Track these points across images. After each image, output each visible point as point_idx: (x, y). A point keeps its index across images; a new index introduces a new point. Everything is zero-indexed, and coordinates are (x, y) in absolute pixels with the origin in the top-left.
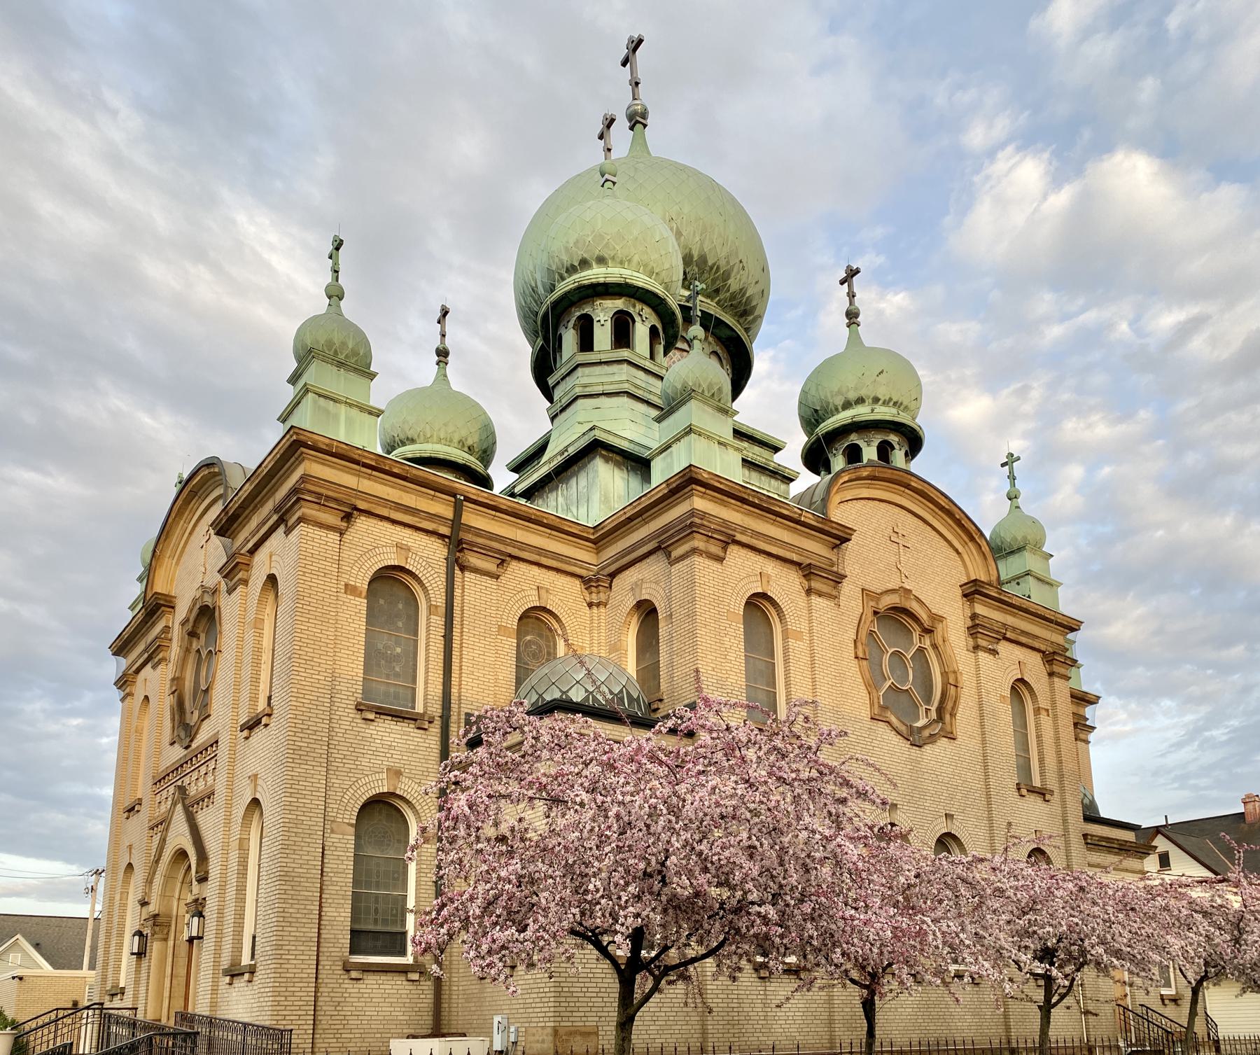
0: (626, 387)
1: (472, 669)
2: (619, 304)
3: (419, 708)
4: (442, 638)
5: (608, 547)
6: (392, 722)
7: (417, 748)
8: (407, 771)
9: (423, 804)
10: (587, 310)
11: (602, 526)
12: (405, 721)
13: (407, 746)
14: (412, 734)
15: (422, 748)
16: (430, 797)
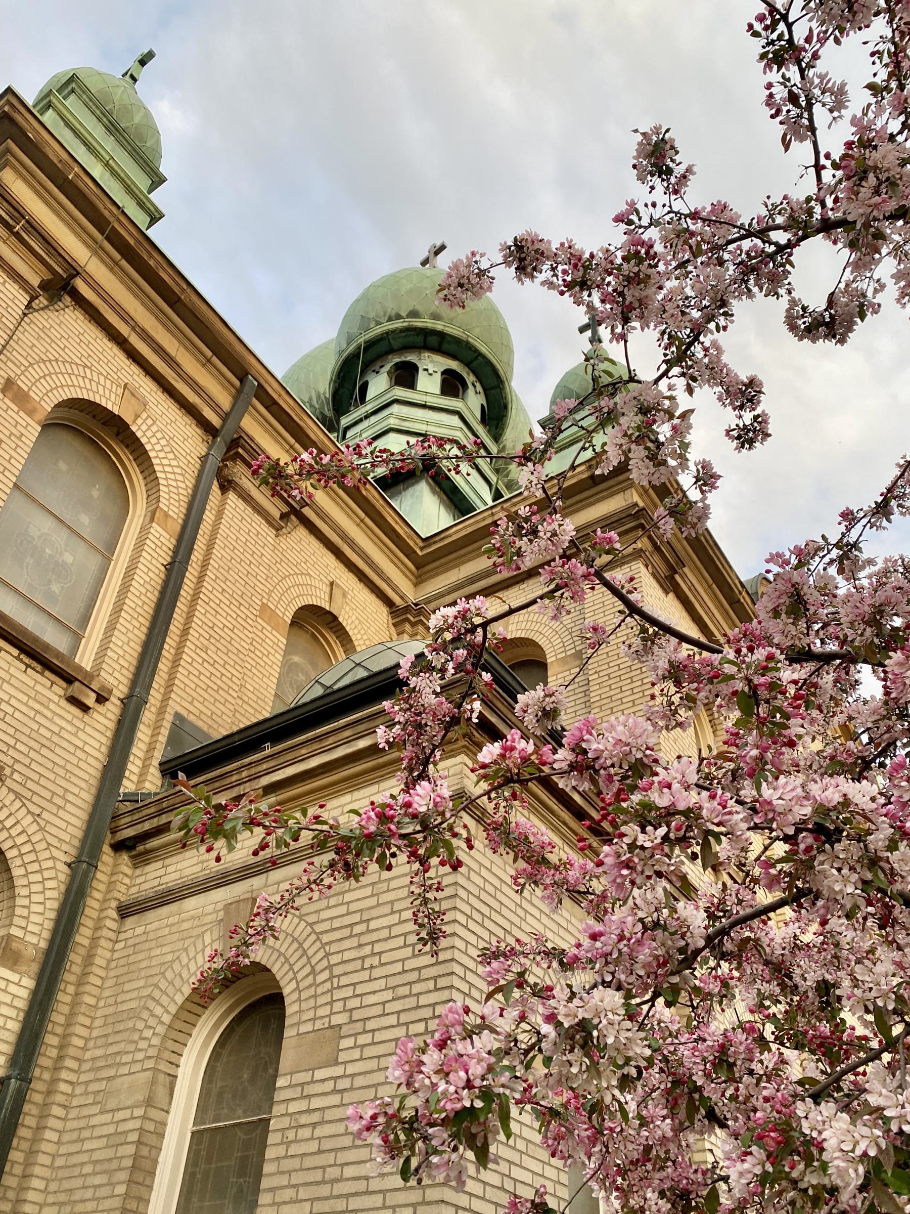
0: (458, 435)
1: (206, 642)
2: (454, 365)
3: (85, 659)
4: (163, 569)
5: (437, 575)
6: (17, 663)
7: (55, 739)
8: (16, 776)
9: (31, 868)
10: (411, 357)
11: (442, 535)
12: (47, 673)
13: (35, 727)
14: (52, 706)
15: (65, 744)
16: (53, 858)
